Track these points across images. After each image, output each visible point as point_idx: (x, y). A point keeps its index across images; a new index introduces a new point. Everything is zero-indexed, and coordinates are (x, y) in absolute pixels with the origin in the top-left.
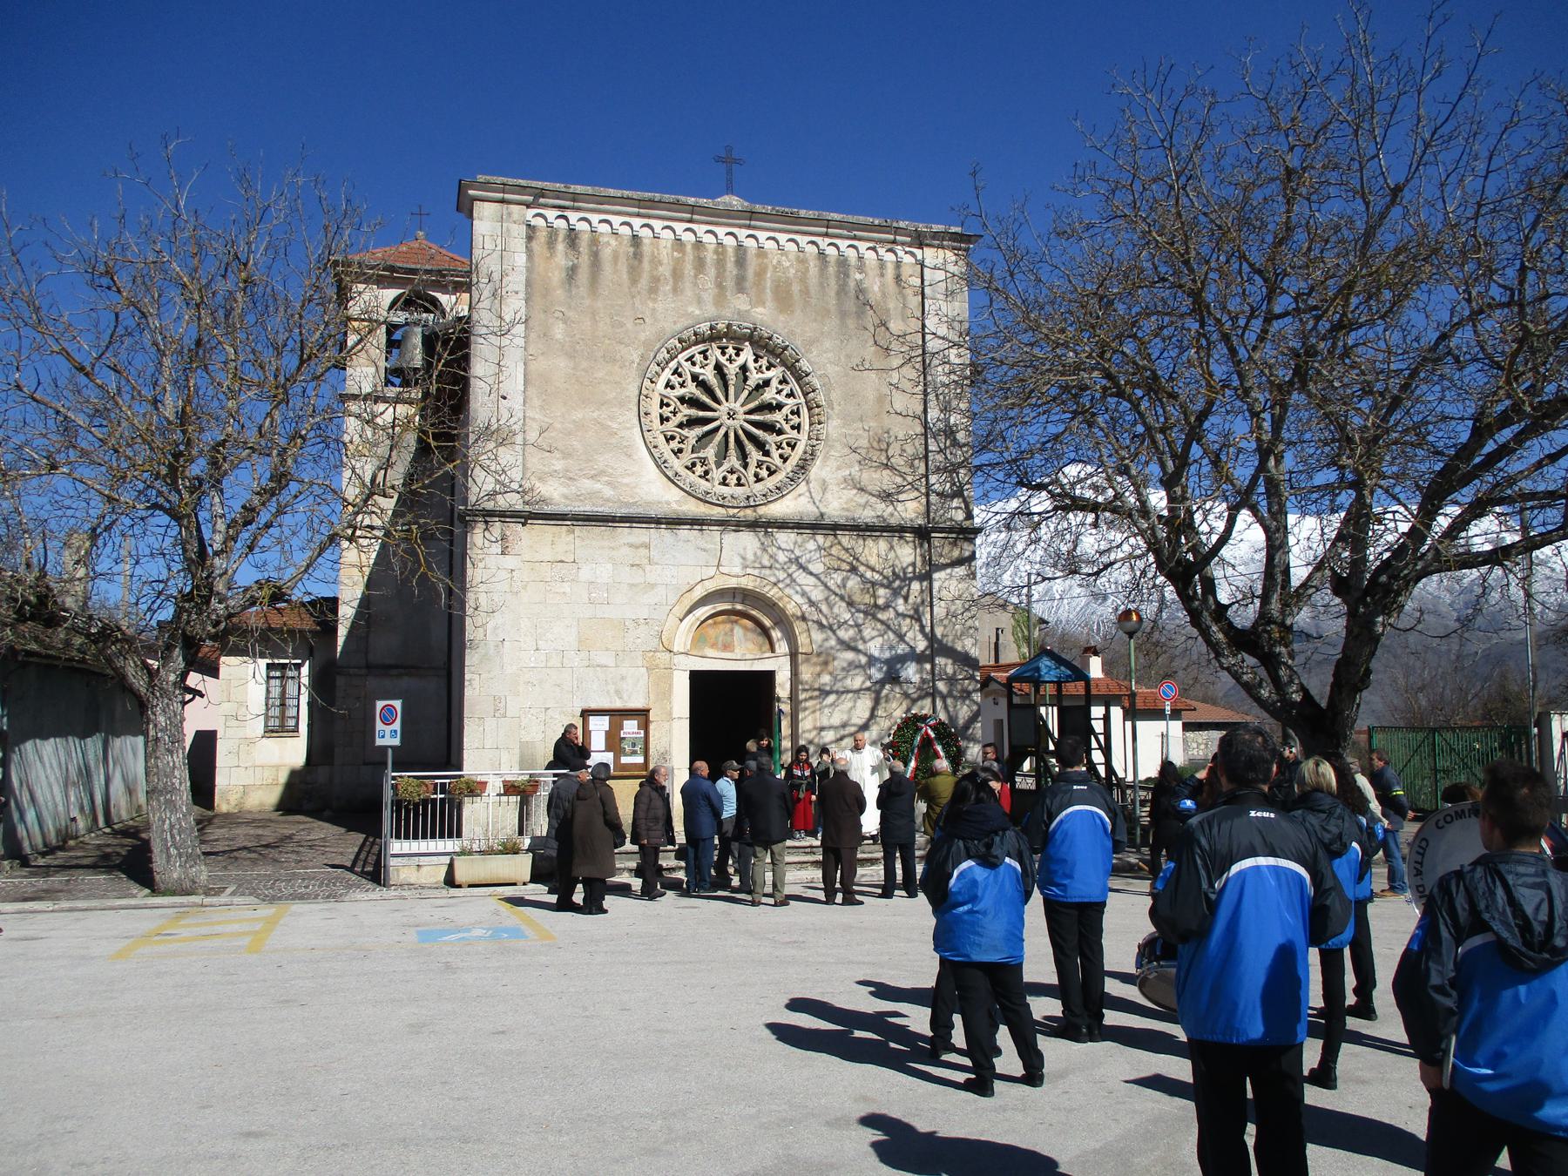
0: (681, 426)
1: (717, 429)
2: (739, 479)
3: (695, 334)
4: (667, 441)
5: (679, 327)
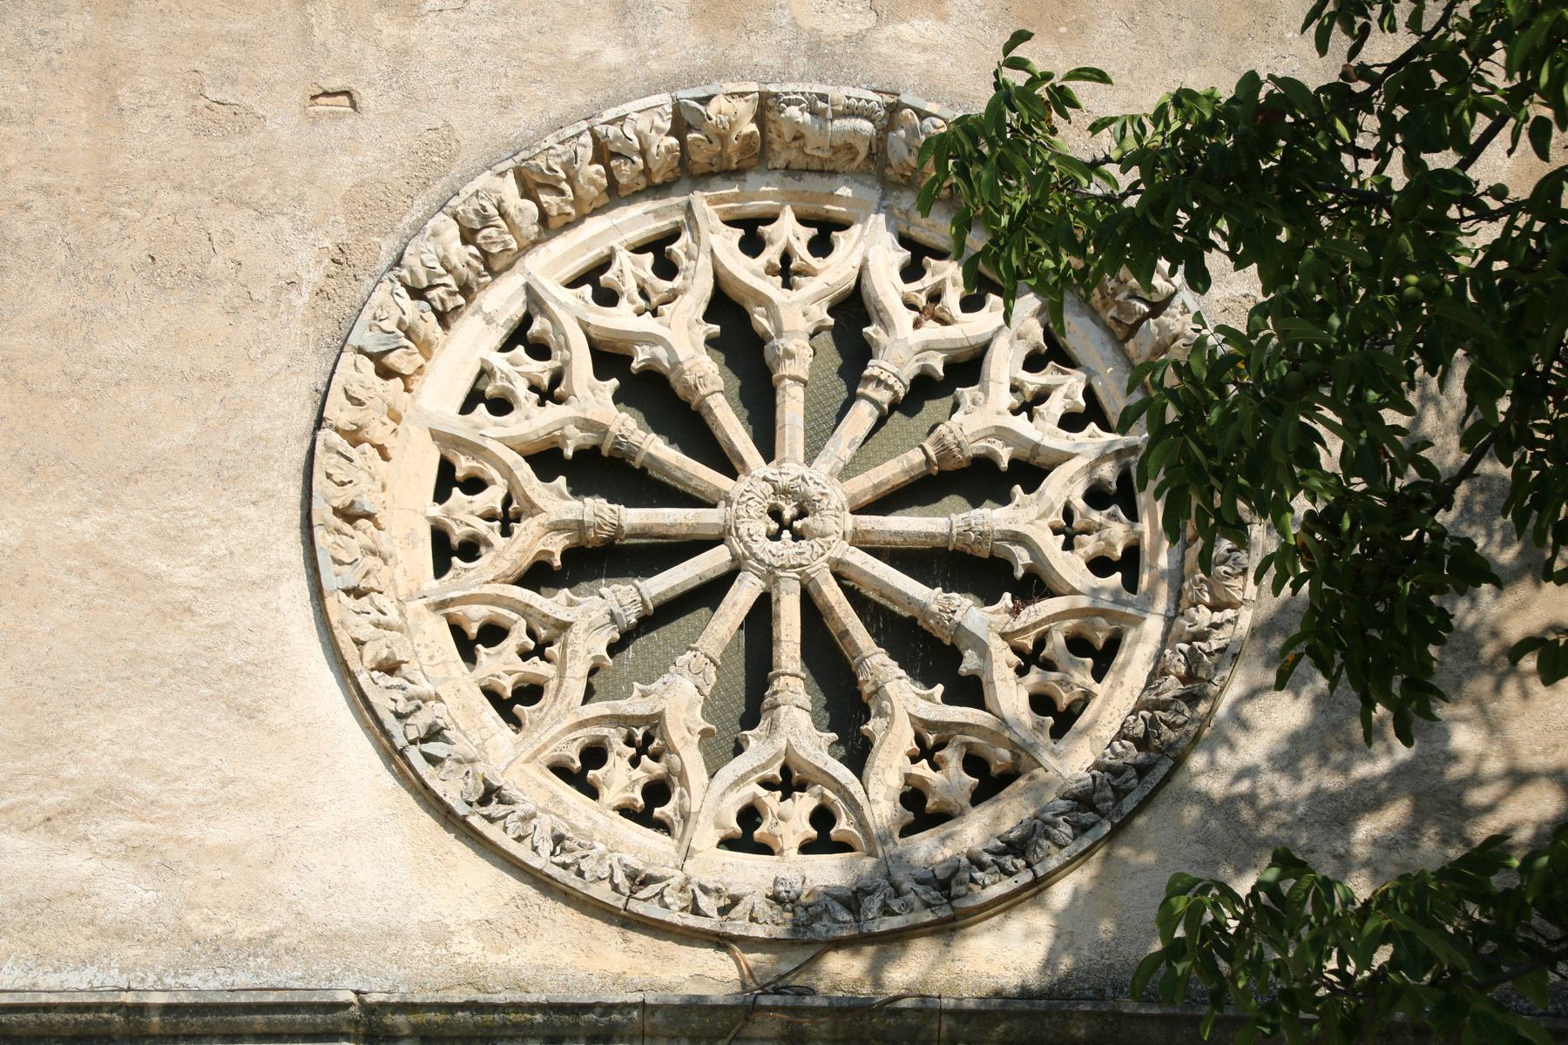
0: (538, 576)
1: (711, 592)
2: (822, 817)
3: (603, 153)
4: (467, 650)
5: (518, 123)
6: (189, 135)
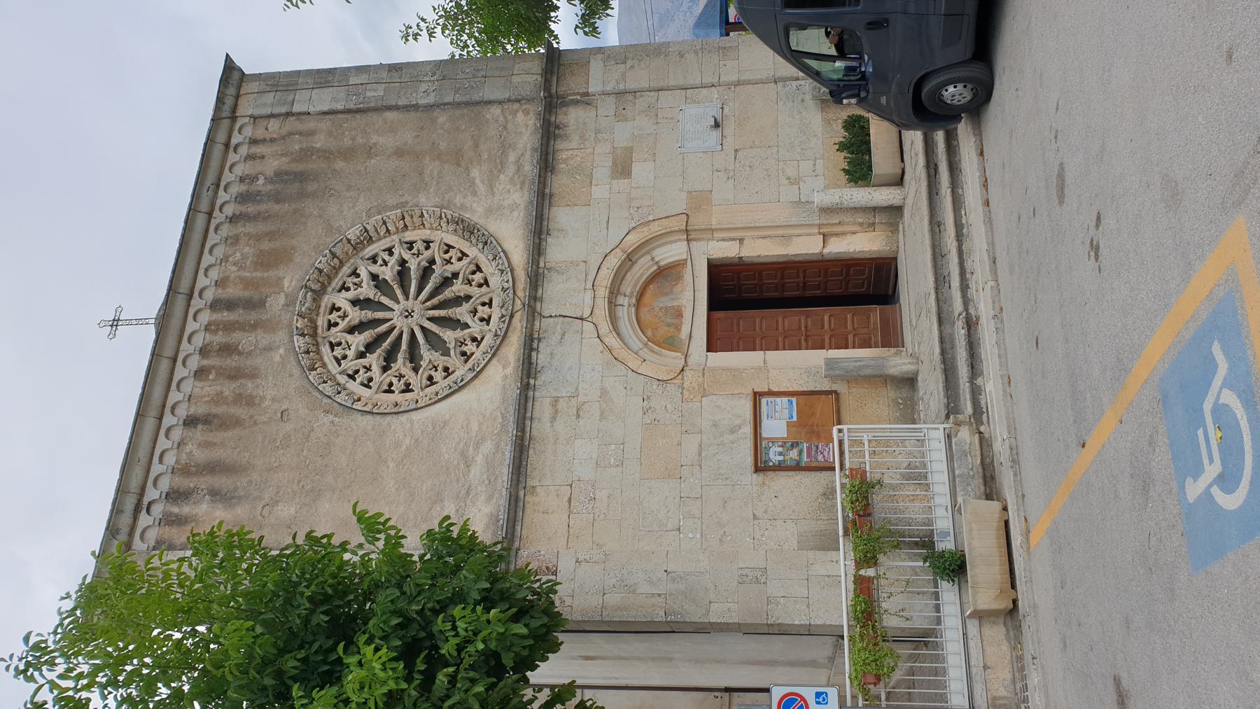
6: (288, 449)
